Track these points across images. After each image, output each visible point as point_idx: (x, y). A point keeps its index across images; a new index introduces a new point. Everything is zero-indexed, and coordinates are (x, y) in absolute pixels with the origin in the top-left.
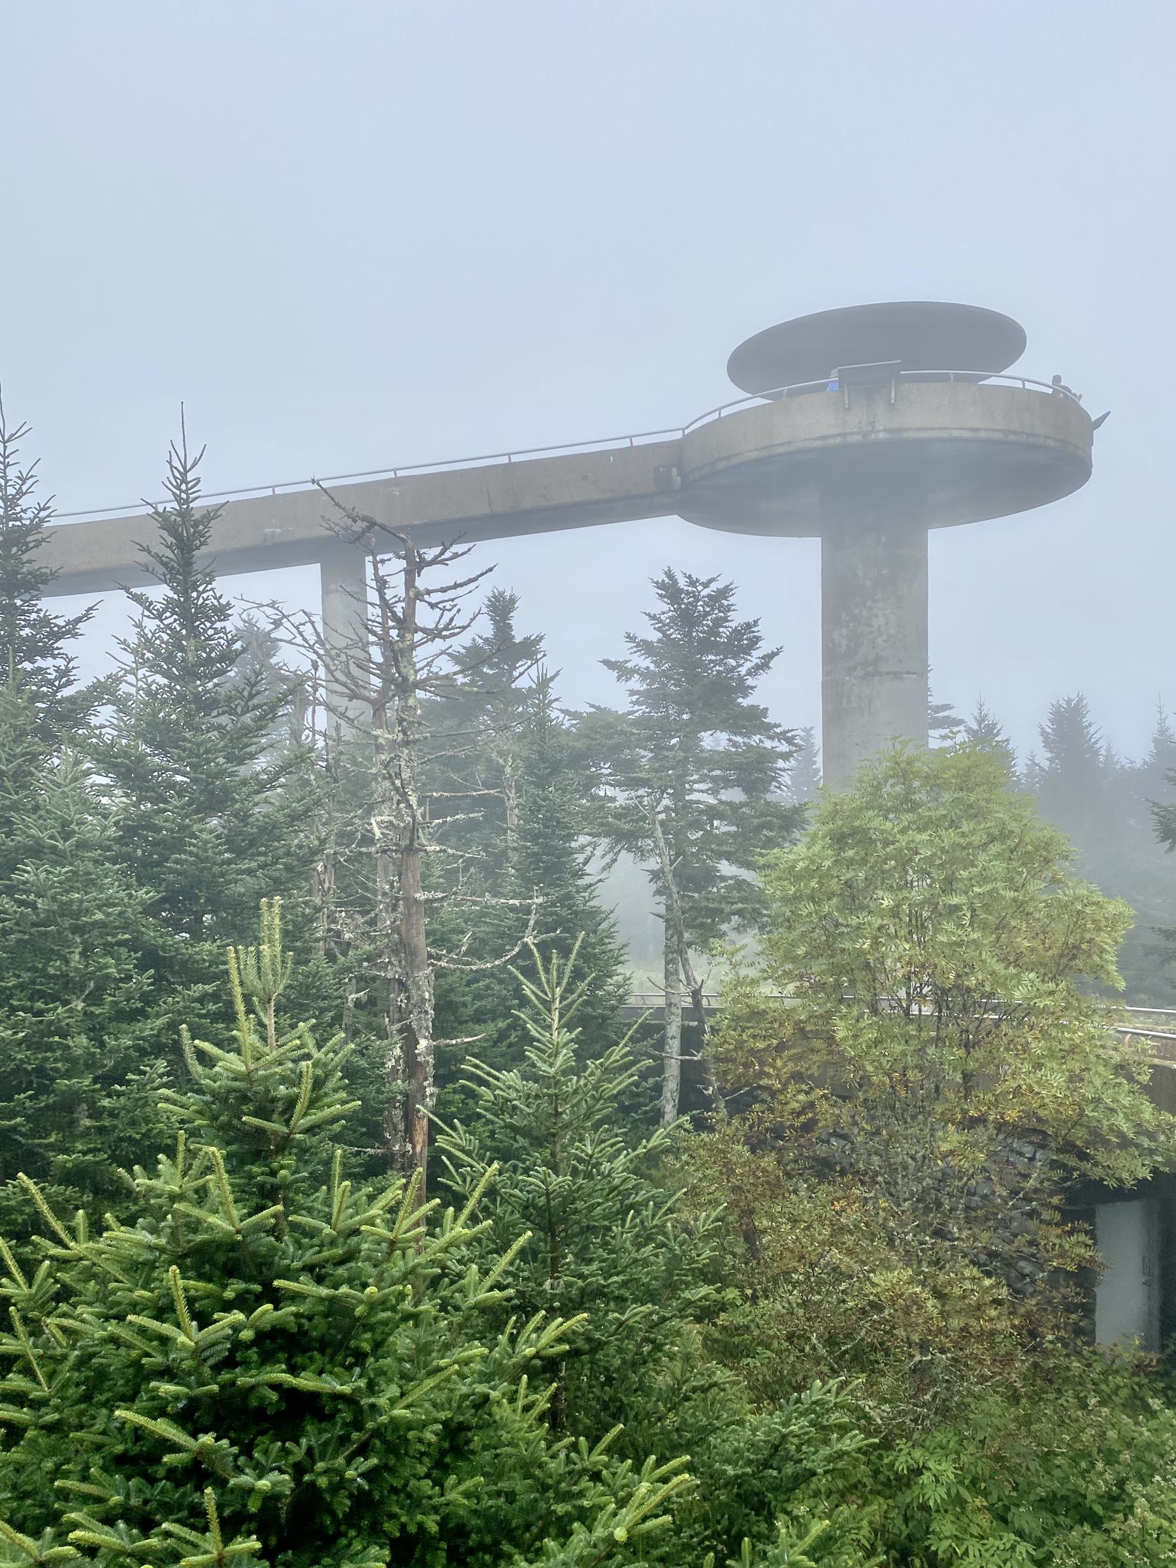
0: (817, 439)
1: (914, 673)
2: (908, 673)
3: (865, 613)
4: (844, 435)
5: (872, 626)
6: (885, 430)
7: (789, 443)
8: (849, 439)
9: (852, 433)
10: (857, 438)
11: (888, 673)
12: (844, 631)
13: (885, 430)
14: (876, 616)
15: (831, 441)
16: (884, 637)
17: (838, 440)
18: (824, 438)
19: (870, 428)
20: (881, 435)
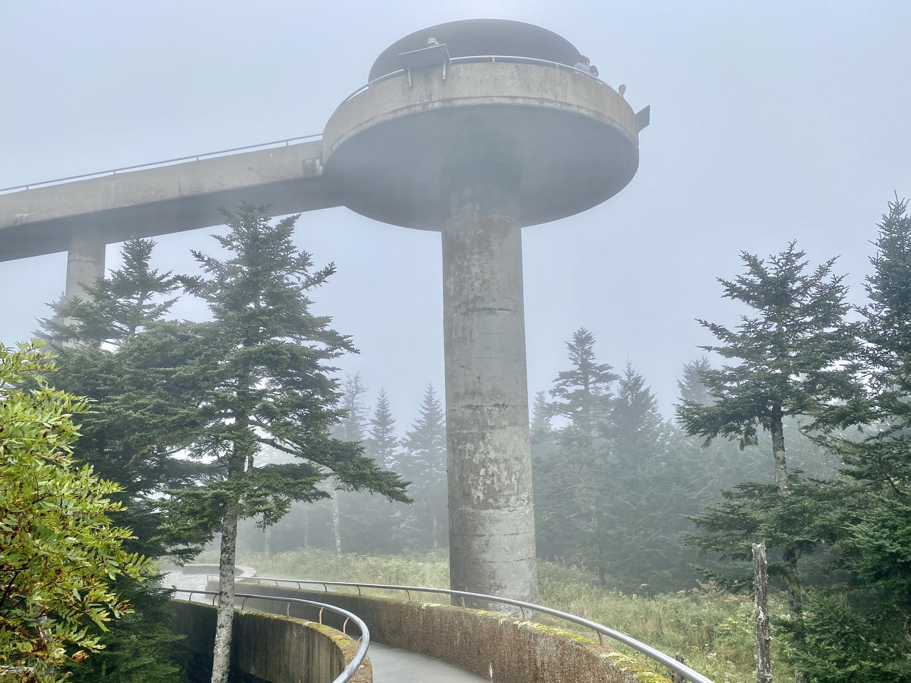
0: (391, 113)
1: (506, 310)
2: (502, 309)
3: (466, 264)
4: (410, 107)
5: (471, 273)
6: (439, 101)
7: (372, 119)
8: (413, 109)
9: (414, 106)
10: (419, 109)
11: (484, 309)
12: (452, 279)
13: (439, 101)
14: (474, 266)
15: (400, 114)
16: (480, 282)
17: (405, 112)
18: (395, 111)
19: (428, 100)
20: (437, 105)
